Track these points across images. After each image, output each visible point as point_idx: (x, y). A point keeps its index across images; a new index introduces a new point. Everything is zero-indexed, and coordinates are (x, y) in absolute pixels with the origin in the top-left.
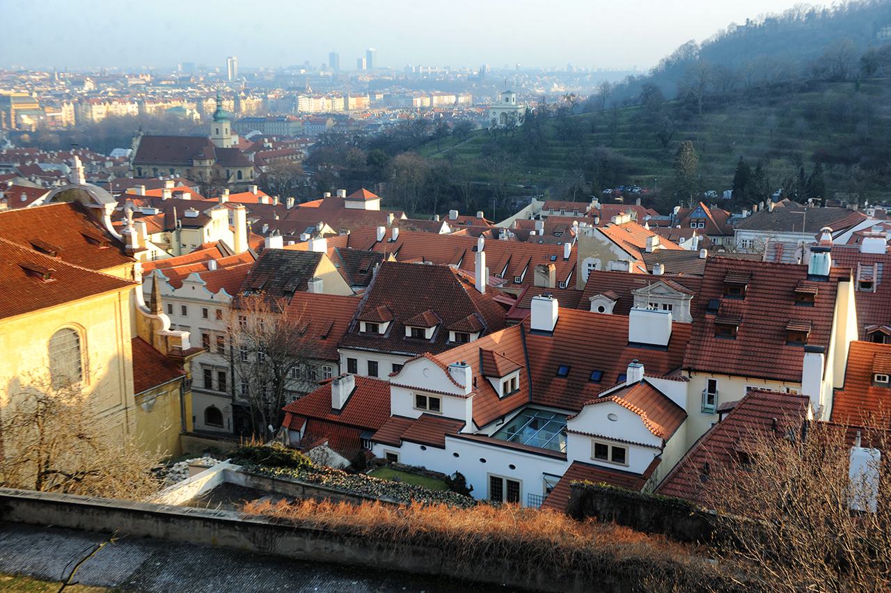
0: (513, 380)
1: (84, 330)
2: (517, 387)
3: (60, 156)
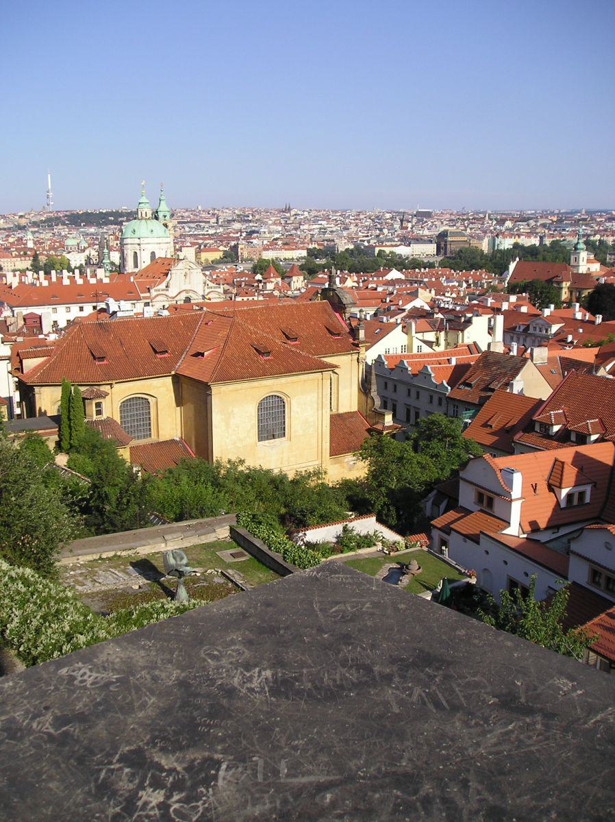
0: (582, 495)
1: (289, 399)
2: (587, 500)
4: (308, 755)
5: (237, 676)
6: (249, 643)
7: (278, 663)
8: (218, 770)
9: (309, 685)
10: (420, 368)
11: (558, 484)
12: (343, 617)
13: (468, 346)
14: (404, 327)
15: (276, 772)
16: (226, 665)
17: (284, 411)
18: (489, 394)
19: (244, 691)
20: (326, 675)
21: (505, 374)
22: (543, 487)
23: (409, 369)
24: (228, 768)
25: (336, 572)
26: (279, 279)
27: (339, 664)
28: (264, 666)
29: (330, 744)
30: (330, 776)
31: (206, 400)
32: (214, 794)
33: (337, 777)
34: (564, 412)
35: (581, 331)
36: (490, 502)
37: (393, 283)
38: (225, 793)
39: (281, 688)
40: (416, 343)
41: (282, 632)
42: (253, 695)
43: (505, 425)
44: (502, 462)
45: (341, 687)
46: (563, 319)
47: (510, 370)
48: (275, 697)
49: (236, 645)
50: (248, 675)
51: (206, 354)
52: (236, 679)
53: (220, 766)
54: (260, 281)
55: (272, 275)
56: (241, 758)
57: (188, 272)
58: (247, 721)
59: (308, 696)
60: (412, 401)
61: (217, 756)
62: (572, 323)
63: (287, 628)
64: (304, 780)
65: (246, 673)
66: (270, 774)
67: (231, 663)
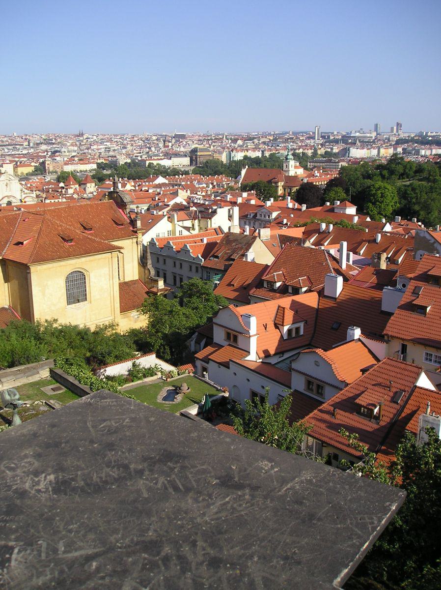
0: (298, 329)
2: (302, 333)
3: (209, 180)
4: (80, 535)
5: (28, 481)
6: (38, 456)
7: (60, 468)
8: (11, 554)
9: (82, 483)
10: (182, 246)
11: (282, 324)
12: (109, 431)
13: (215, 229)
14: (169, 218)
15: (55, 551)
16: (20, 474)
17: (85, 282)
18: (231, 262)
19: (33, 492)
20: (95, 475)
21: (241, 248)
22: (271, 326)
23: (174, 247)
24: (19, 552)
25: (105, 398)
26: (77, 186)
27: (104, 466)
28: (50, 472)
29: (96, 525)
30: (96, 549)
31: (27, 276)
32: (8, 573)
33: (101, 549)
34: (283, 273)
35: (292, 216)
36: (235, 339)
37: (159, 186)
38: (16, 571)
39: (60, 487)
40: (178, 229)
41: (63, 445)
42: (40, 494)
43: (243, 284)
44: (242, 310)
45: (106, 482)
46: (280, 208)
47: (245, 245)
48: (56, 495)
49: (27, 458)
50: (37, 480)
51: (25, 243)
52: (27, 484)
53: (13, 551)
54: (63, 188)
55: (72, 183)
56: (30, 543)
57: (8, 182)
58: (35, 514)
59: (82, 492)
60: (177, 270)
61: (11, 544)
62: (286, 210)
63: (67, 442)
64: (77, 554)
65: (35, 478)
66: (51, 553)
67: (24, 472)
